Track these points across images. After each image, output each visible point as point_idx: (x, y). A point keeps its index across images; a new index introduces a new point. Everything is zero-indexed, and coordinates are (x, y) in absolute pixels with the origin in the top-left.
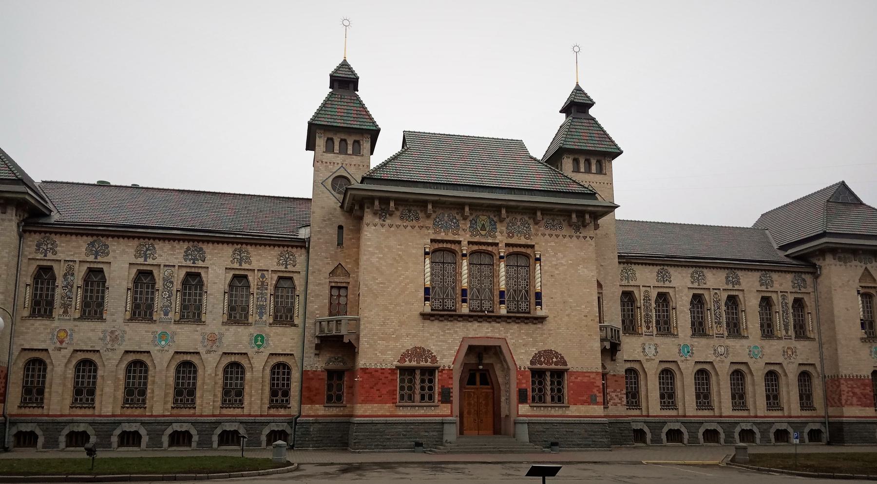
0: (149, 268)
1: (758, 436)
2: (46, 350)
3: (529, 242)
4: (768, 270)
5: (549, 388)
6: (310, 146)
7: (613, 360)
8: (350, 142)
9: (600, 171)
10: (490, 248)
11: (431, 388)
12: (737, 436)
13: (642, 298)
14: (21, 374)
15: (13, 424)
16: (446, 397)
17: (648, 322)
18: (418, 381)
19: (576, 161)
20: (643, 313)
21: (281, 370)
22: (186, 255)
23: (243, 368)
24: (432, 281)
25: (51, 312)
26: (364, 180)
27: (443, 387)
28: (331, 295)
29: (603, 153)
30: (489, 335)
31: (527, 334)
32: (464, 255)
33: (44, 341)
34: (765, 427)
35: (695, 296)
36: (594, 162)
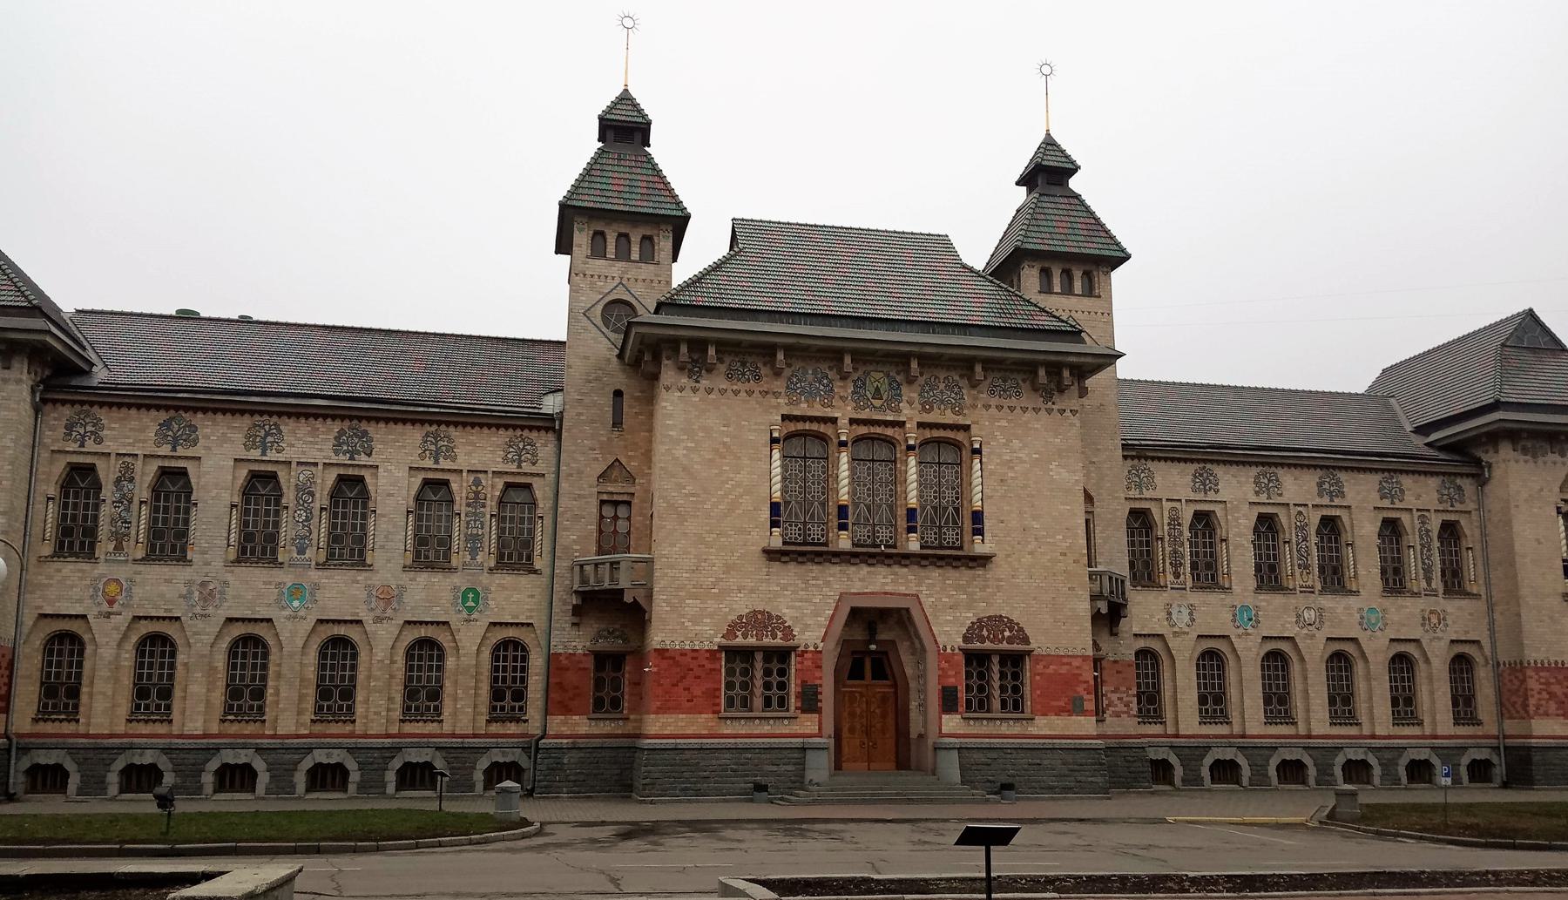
0: (270, 468)
1: (1377, 771)
2: (84, 617)
3: (961, 420)
4: (1395, 471)
5: (996, 684)
6: (563, 244)
7: (1113, 634)
8: (635, 239)
9: (1089, 292)
10: (889, 432)
11: (782, 686)
12: (1338, 771)
13: (1166, 521)
14: (37, 660)
15: (24, 750)
16: (810, 702)
17: (1177, 565)
18: (759, 673)
19: (1046, 273)
20: (1168, 549)
21: (510, 653)
22: (338, 442)
23: (440, 648)
24: (784, 490)
25: (92, 546)
26: (660, 307)
27: (804, 683)
28: (602, 517)
29: (1097, 259)
30: (888, 589)
31: (957, 588)
32: (843, 444)
33: (80, 601)
34: (1388, 755)
35: (1262, 518)
36: (1077, 274)
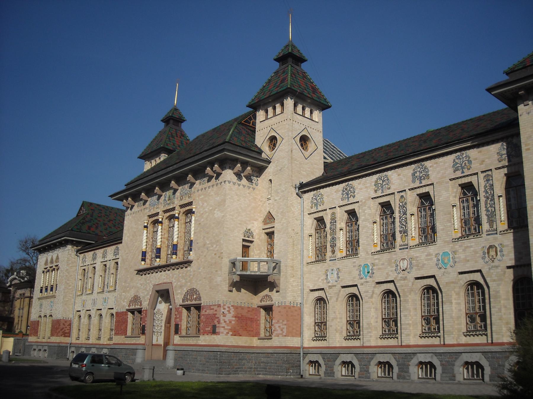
30: (165, 281)
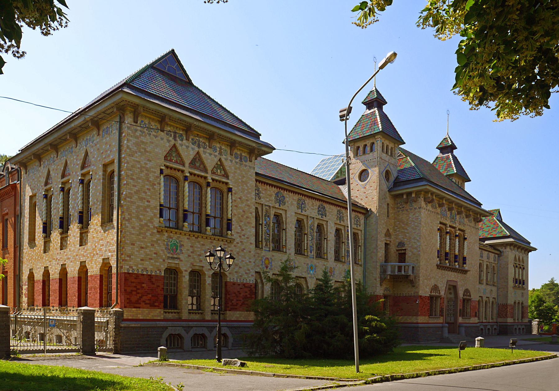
33: (258, 266)
